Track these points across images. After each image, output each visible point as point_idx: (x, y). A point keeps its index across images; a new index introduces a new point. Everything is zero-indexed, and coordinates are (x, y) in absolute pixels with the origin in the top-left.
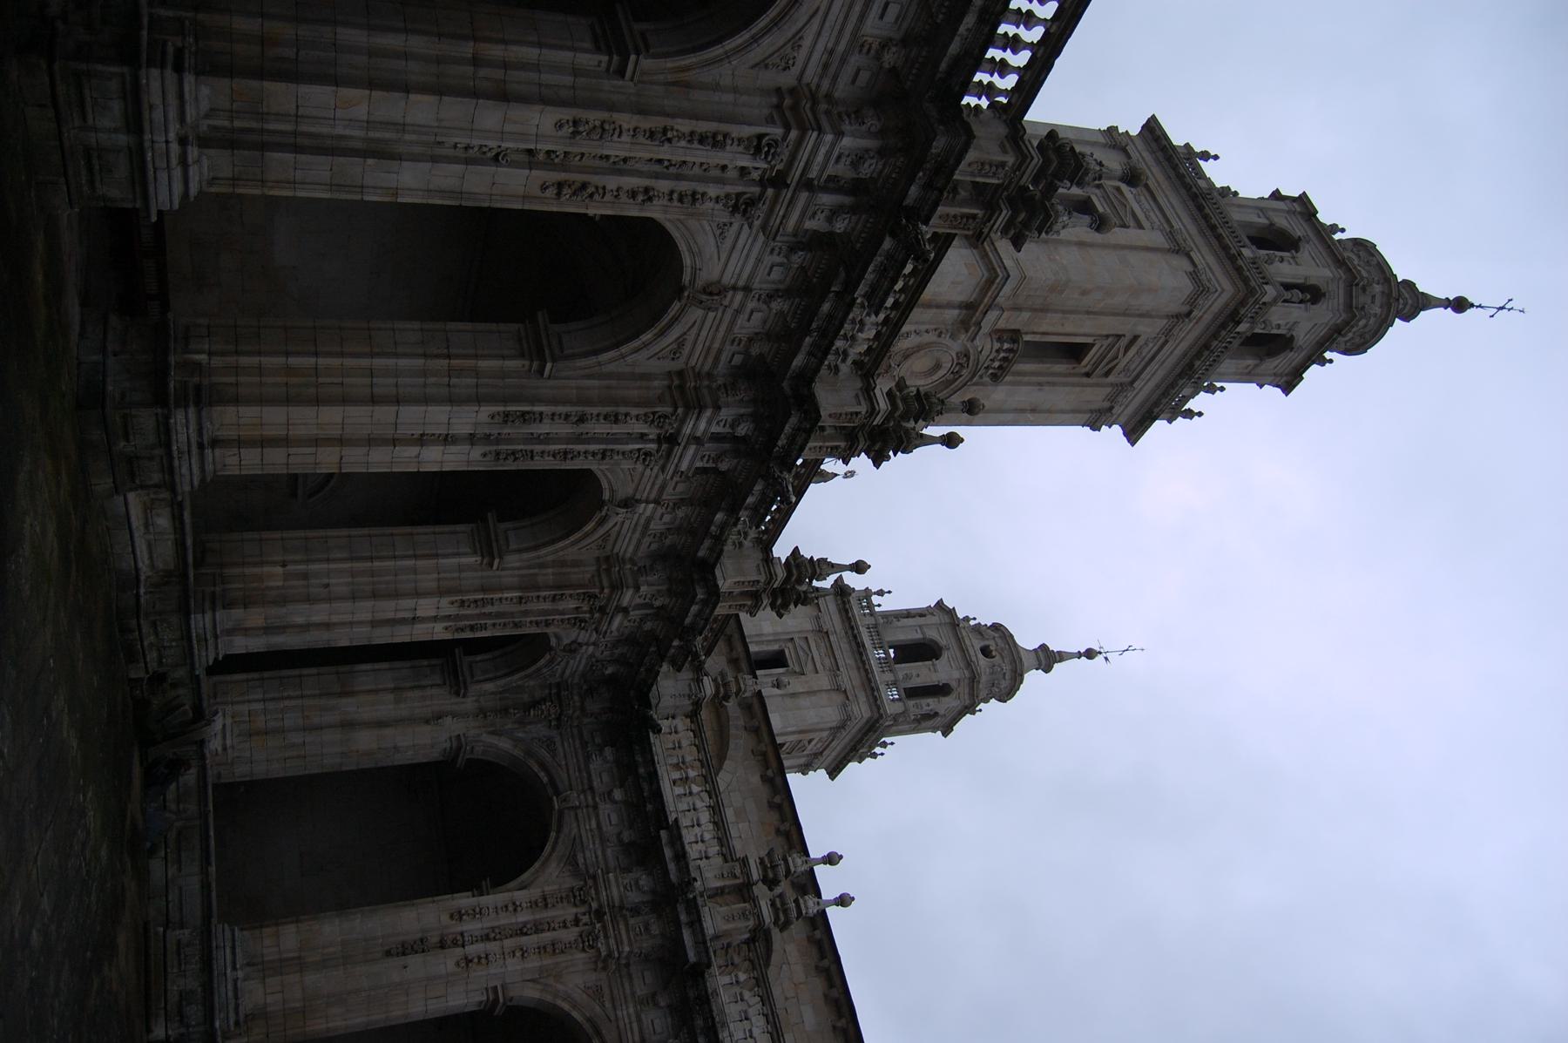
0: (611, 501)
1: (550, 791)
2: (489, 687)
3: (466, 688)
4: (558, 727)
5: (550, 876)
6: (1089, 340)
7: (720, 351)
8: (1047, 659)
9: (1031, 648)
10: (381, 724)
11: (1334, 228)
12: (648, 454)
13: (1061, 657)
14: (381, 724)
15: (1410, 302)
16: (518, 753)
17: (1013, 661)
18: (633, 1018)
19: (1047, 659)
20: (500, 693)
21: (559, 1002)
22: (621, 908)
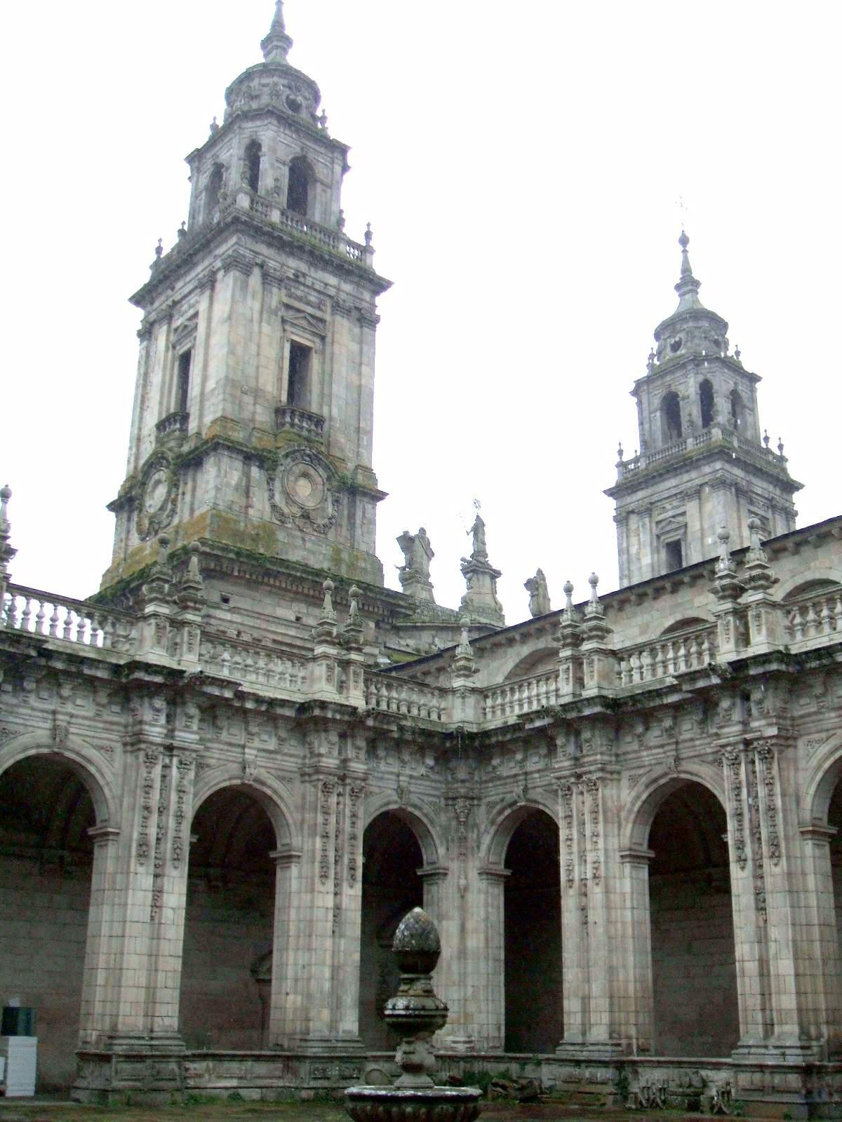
0: (242, 778)
1: (515, 808)
2: (442, 851)
3: (438, 869)
4: (479, 799)
5: (558, 811)
6: (287, 347)
7: (105, 722)
8: (688, 284)
9: (678, 299)
10: (463, 929)
11: (214, 127)
12: (181, 762)
13: (686, 270)
14: (463, 929)
15: (275, 43)
16: (492, 830)
17: (684, 320)
18: (650, 752)
19: (688, 284)
20: (447, 841)
21: (636, 809)
22: (576, 759)
